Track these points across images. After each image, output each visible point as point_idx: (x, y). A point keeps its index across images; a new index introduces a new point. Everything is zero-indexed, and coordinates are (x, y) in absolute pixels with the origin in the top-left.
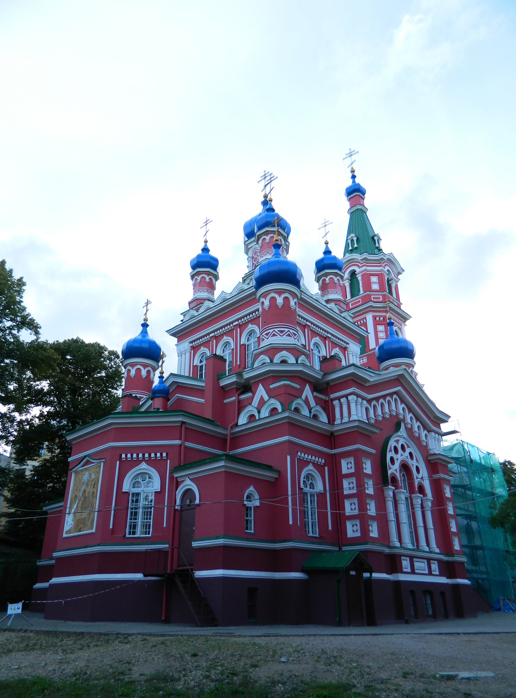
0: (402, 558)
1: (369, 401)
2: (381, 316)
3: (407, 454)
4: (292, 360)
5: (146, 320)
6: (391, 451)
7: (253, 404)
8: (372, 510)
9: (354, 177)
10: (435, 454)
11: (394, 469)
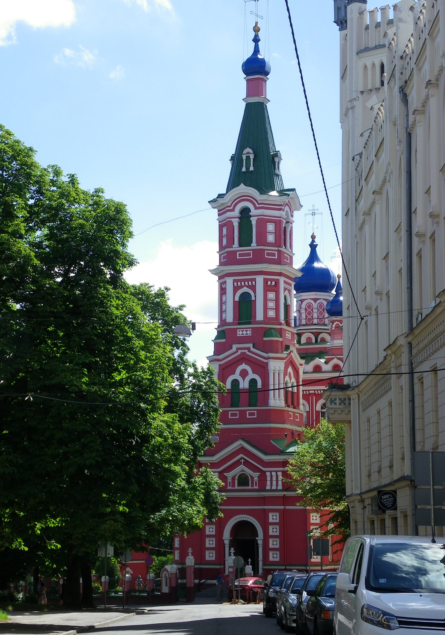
9: (256, 40)
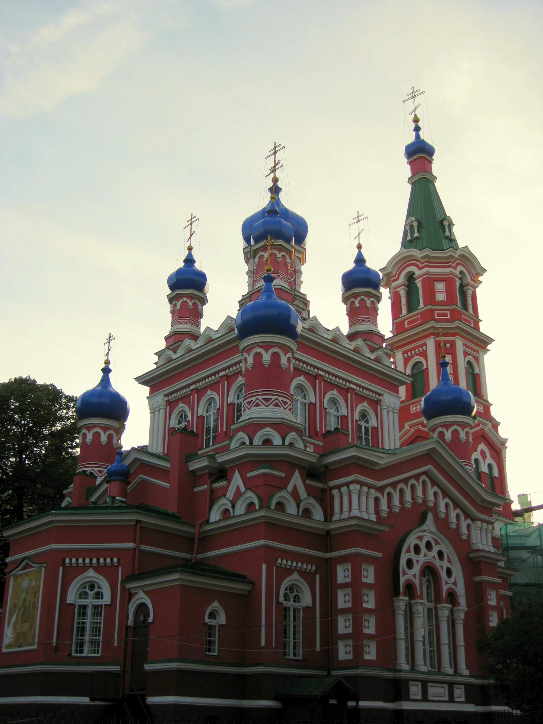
0: (411, 683)
1: (381, 489)
2: (448, 342)
3: (434, 552)
4: (277, 440)
5: (107, 362)
6: (408, 551)
7: (227, 496)
8: (370, 627)
9: (417, 129)
10: (478, 550)
11: (410, 575)
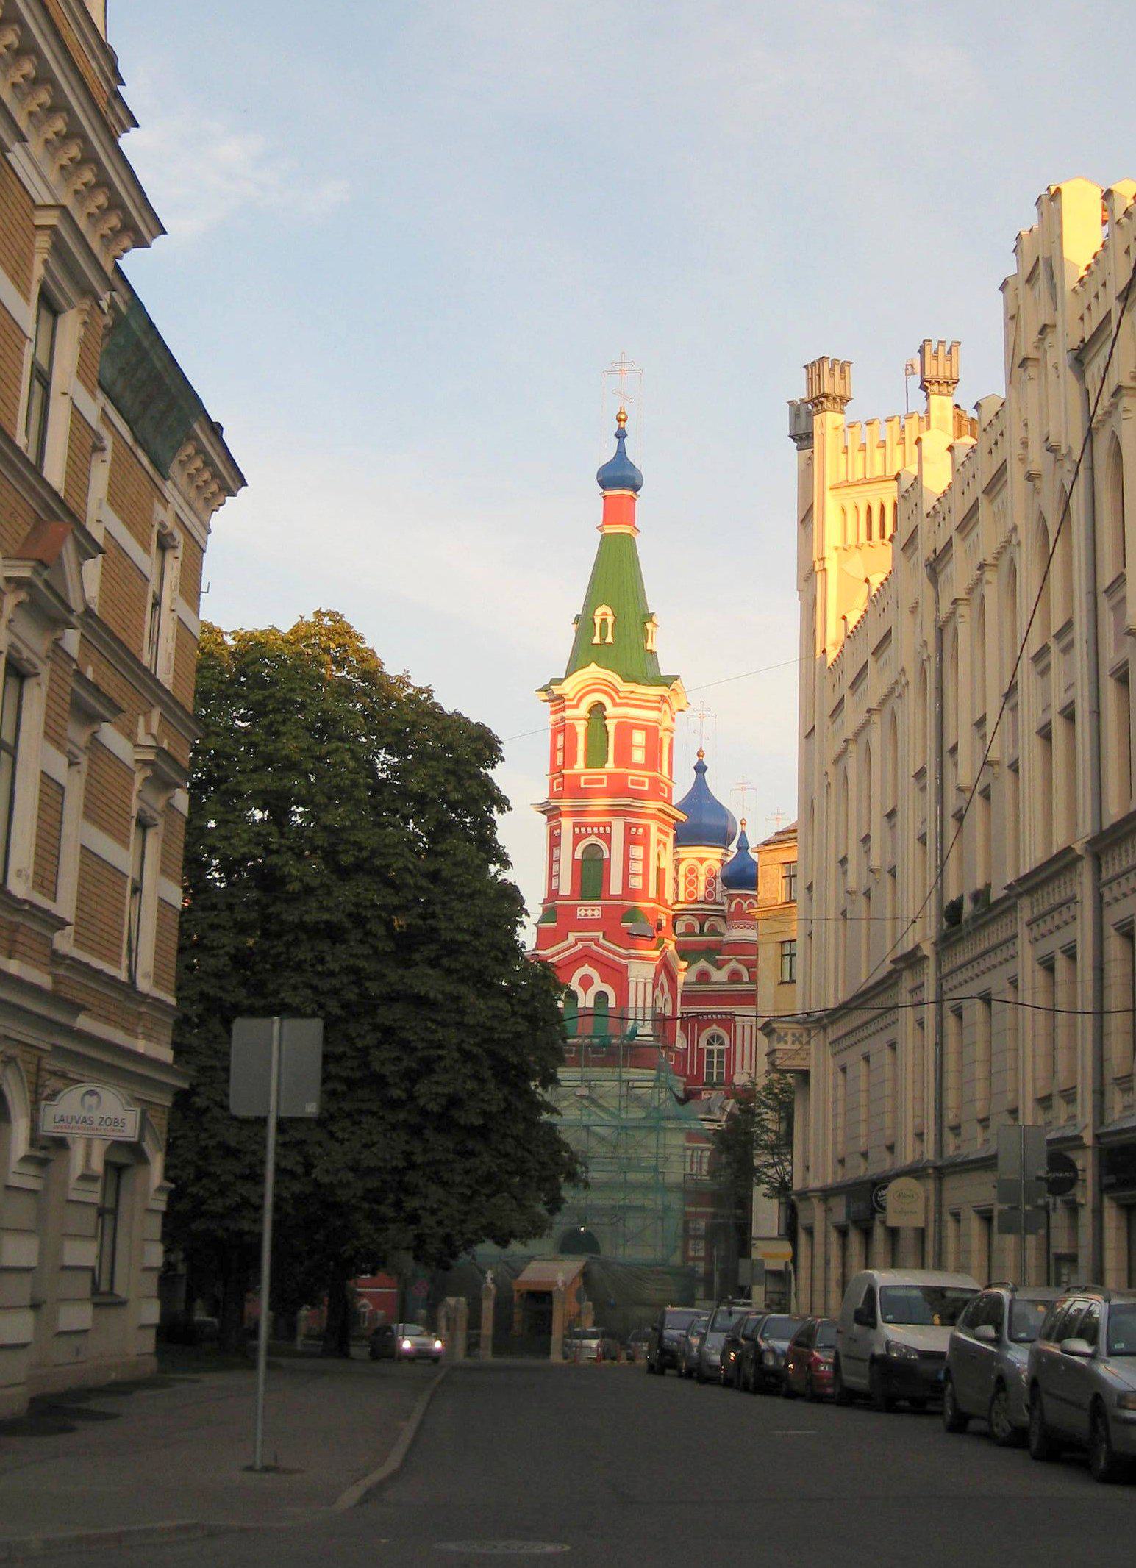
9: (621, 435)
